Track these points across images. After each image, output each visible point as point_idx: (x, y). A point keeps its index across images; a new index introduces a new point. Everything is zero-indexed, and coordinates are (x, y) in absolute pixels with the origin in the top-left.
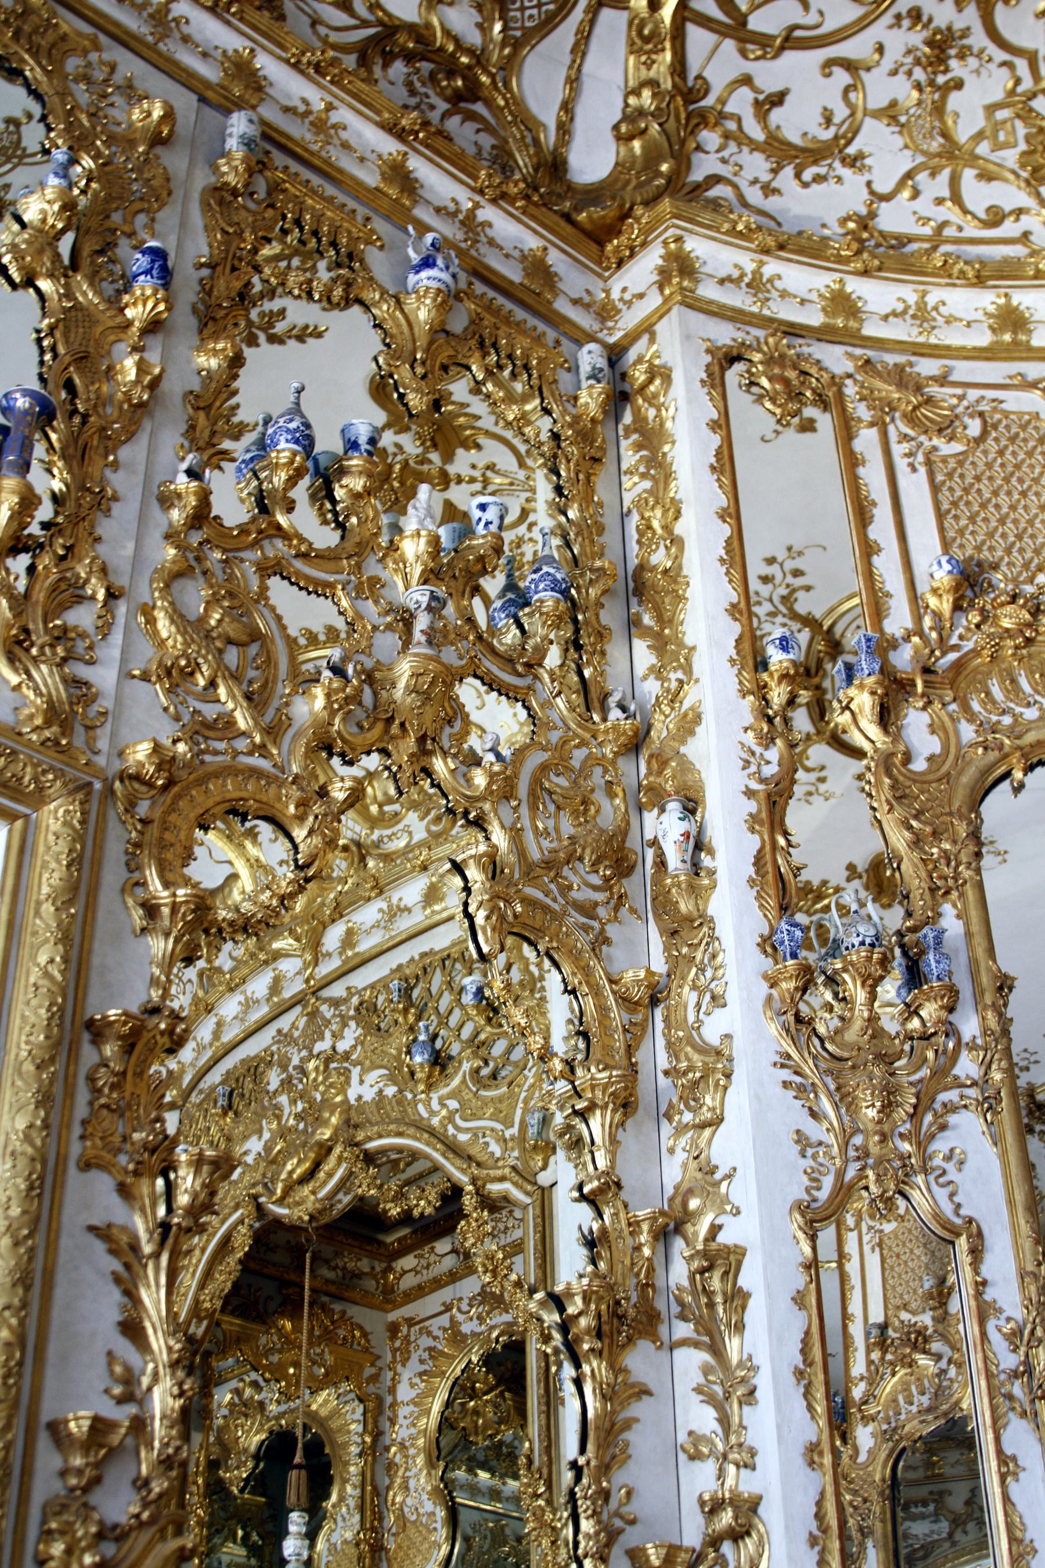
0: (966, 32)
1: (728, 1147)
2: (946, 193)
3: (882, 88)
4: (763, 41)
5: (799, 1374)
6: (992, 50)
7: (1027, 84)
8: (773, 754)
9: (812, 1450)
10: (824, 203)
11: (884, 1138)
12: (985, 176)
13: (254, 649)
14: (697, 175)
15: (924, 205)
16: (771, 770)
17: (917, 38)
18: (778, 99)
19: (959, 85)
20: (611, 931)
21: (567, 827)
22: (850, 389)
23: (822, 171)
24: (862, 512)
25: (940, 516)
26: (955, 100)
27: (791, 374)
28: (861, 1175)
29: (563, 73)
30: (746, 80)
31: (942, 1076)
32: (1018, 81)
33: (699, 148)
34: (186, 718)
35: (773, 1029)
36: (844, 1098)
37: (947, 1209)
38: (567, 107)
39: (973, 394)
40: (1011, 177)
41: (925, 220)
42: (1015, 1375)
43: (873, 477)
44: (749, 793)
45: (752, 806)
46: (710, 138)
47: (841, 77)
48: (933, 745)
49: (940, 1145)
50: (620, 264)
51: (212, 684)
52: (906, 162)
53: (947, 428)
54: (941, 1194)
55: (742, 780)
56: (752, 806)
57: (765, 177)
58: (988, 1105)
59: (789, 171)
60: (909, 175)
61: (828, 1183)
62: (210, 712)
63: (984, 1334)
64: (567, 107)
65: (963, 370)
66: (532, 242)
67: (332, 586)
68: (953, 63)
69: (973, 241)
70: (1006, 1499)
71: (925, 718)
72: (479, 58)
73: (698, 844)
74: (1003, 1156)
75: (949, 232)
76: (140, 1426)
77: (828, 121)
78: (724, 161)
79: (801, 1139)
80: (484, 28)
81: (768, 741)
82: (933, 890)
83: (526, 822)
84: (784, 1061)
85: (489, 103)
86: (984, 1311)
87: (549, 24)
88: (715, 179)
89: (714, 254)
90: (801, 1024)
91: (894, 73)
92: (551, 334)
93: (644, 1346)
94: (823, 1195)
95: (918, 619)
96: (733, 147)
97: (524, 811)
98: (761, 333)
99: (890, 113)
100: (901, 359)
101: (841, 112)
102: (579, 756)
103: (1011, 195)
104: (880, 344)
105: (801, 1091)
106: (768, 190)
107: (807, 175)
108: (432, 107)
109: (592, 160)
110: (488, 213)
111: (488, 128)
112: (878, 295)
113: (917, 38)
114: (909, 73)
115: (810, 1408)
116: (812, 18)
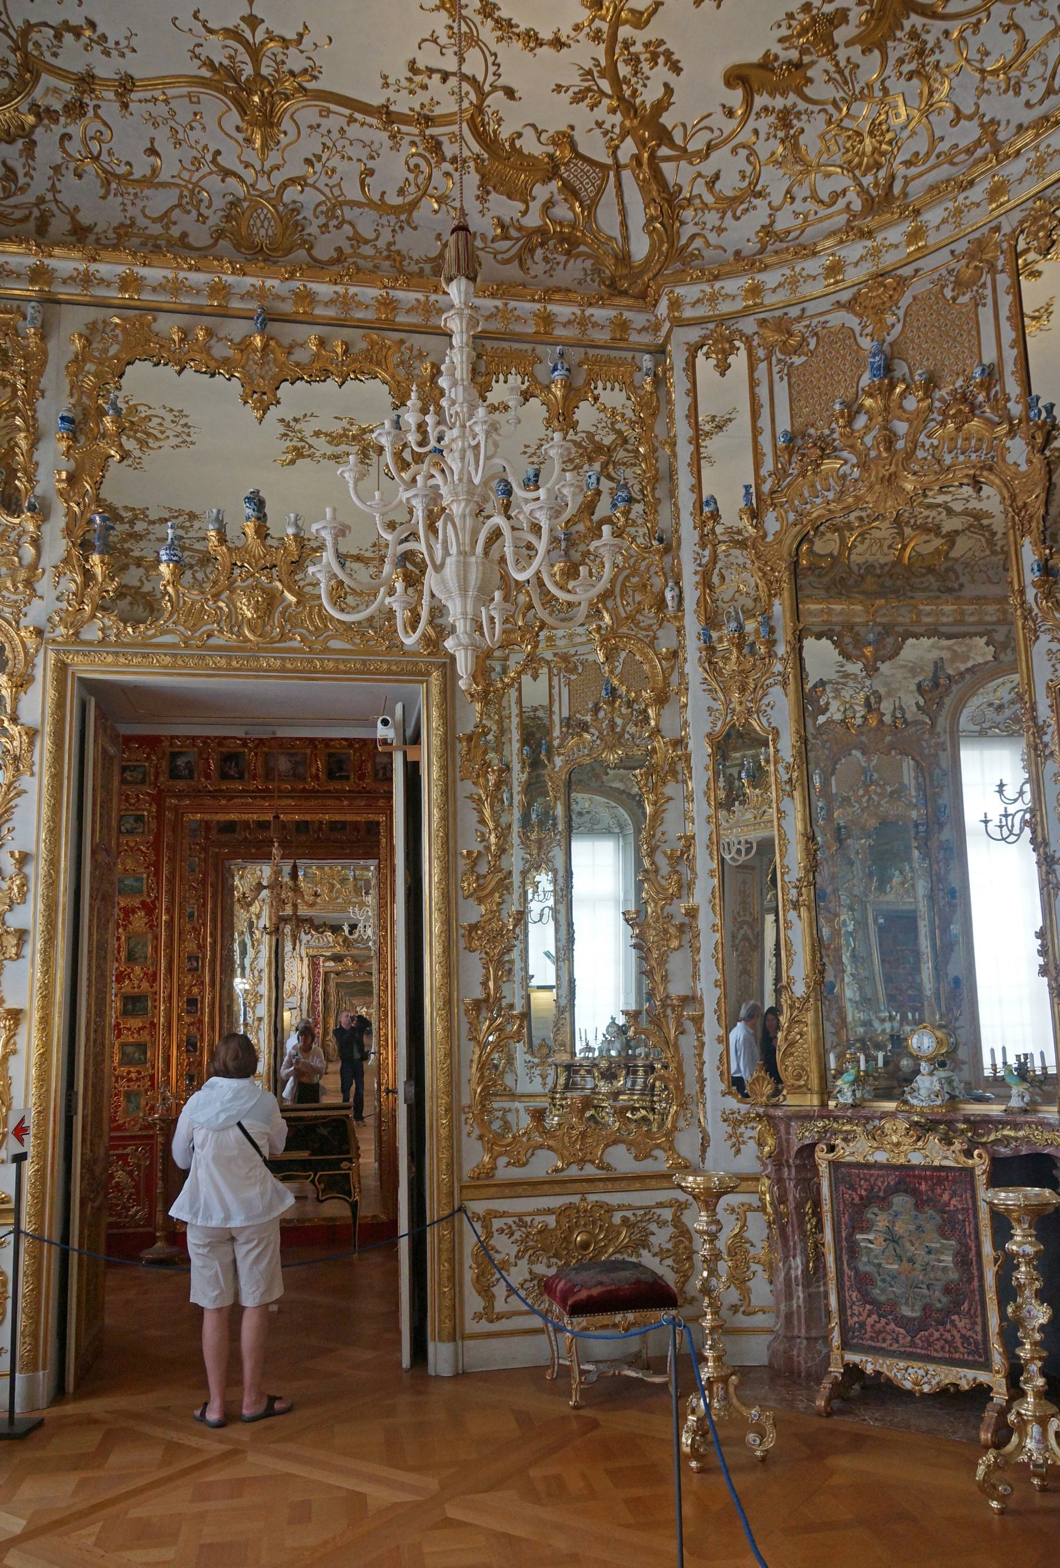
0: (795, 105)
1: (689, 714)
2: (808, 194)
4: (697, 153)
5: (705, 793)
6: (811, 107)
8: (707, 553)
10: (743, 232)
11: (741, 703)
14: (683, 241)
15: (798, 206)
16: (704, 561)
17: (772, 119)
19: (802, 131)
20: (659, 633)
21: (638, 597)
23: (744, 206)
24: (755, 415)
27: (727, 346)
29: (616, 208)
30: (699, 175)
32: (831, 116)
33: (682, 223)
35: (701, 670)
37: (766, 724)
38: (624, 224)
39: (815, 322)
40: (839, 170)
41: (796, 215)
43: (763, 391)
44: (696, 573)
46: (688, 214)
47: (743, 153)
49: (765, 701)
50: (655, 306)
52: (786, 183)
54: (764, 720)
57: (717, 224)
58: (785, 685)
60: (788, 192)
63: (776, 770)
64: (624, 224)
66: (612, 313)
68: (795, 122)
69: (821, 220)
70: (779, 825)
71: (775, 514)
72: (573, 226)
73: (680, 599)
75: (812, 217)
76: (488, 848)
77: (744, 177)
78: (696, 224)
79: (709, 709)
80: (572, 208)
81: (703, 546)
82: (770, 596)
83: (619, 603)
85: (586, 244)
87: (600, 191)
88: (693, 237)
89: (688, 292)
91: (767, 139)
92: (629, 355)
97: (618, 599)
98: (712, 326)
100: (778, 313)
101: (749, 169)
106: (720, 230)
107: (738, 213)
108: (558, 263)
109: (640, 247)
110: (589, 311)
111: (589, 256)
113: (772, 119)
114: (775, 136)
115: (709, 804)
116: (717, 133)
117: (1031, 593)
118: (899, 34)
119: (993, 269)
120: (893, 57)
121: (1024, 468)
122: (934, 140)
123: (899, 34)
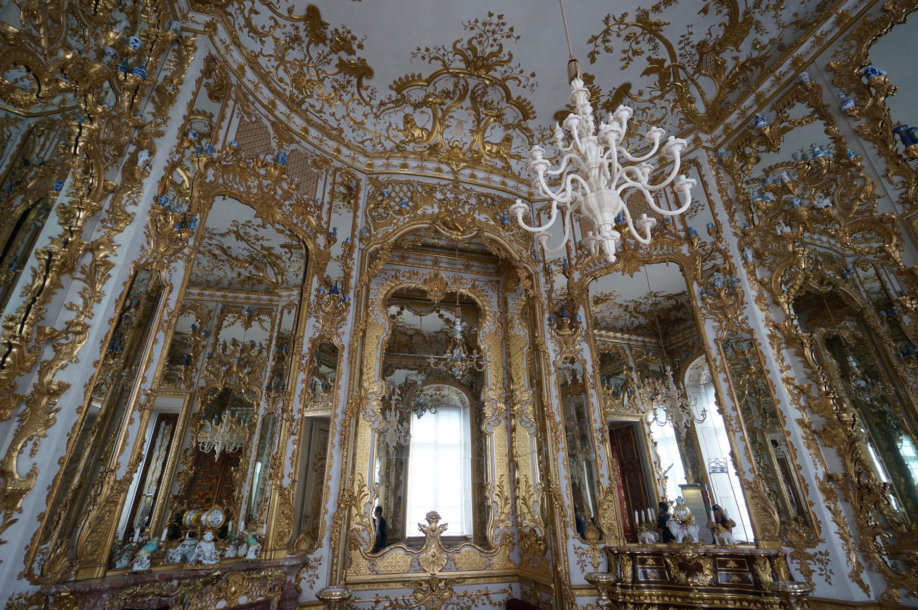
0: (303, 42)
3: (278, 33)
5: (116, 301)
7: (306, 62)
8: (178, 156)
9: (111, 320)
12: (286, 71)
13: (56, 25)
15: (270, 64)
16: (175, 160)
17: (293, 32)
18: (257, 13)
19: (294, 49)
20: (110, 168)
22: (233, 89)
25: (238, 132)
26: (290, 51)
28: (153, 262)
31: (181, 249)
34: (26, 28)
35: (148, 218)
36: (157, 244)
37: (168, 279)
39: (257, 112)
42: (166, 322)
45: (167, 165)
48: (212, 179)
49: (173, 265)
51: (40, 26)
53: (249, 114)
54: (168, 275)
55: (167, 157)
56: (167, 165)
59: (247, 29)
60: (271, 55)
61: (144, 260)
62: (34, 32)
65: (257, 105)
67: (86, 27)
74: (185, 275)
81: (177, 152)
84: (147, 227)
86: (166, 305)
88: (231, 15)
90: (154, 221)
93: (68, 275)
94: (142, 262)
95: (222, 150)
96: (239, 12)
99: (277, 40)
101: (267, 29)
102: (123, 120)
103: (287, 80)
104: (246, 87)
105: (148, 236)
106: (240, 28)
107: (251, 34)
112: (250, 75)
113: (293, 32)
116: (277, 6)
117: (312, 298)
118: (347, 76)
119: (327, 171)
120: (338, 77)
121: (322, 248)
122: (320, 111)
123: (347, 76)
